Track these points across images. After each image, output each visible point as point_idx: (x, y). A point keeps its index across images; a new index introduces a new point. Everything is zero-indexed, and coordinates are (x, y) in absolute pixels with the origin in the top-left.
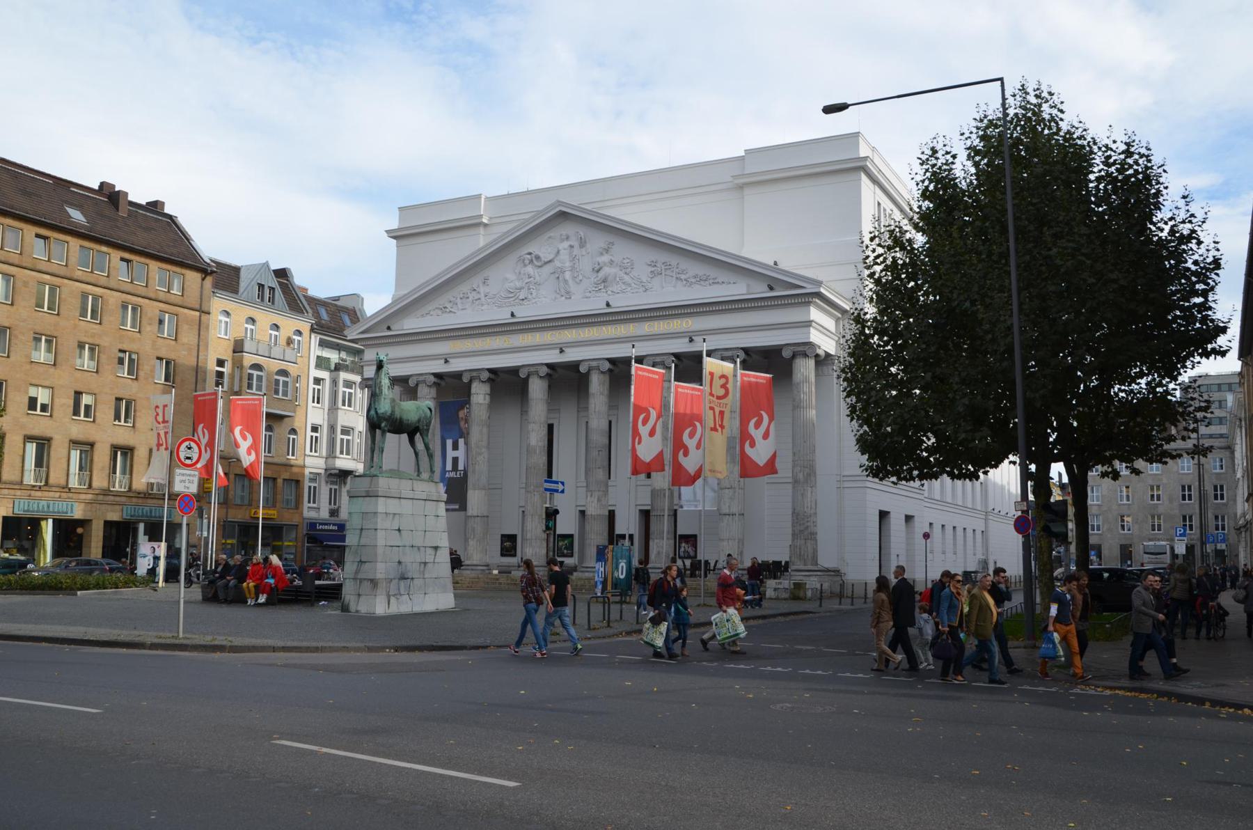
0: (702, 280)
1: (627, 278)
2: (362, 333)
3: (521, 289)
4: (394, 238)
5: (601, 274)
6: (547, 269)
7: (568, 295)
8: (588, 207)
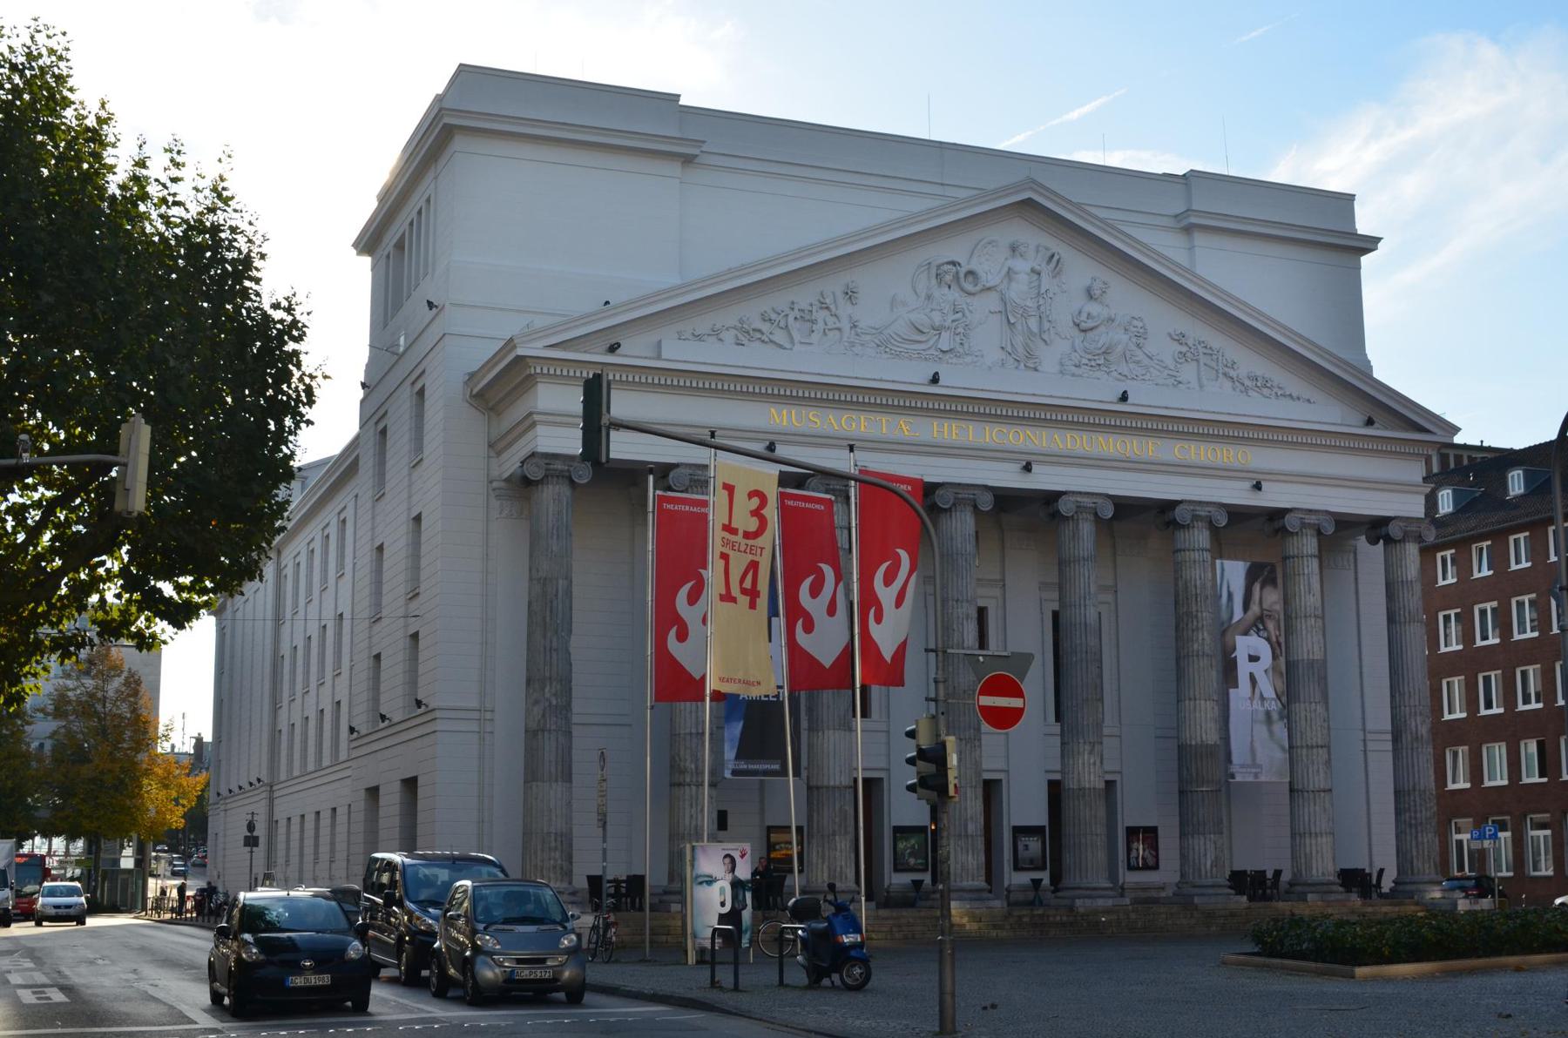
0: (1262, 385)
3: (938, 330)
5: (1103, 338)
6: (991, 302)
7: (1028, 361)
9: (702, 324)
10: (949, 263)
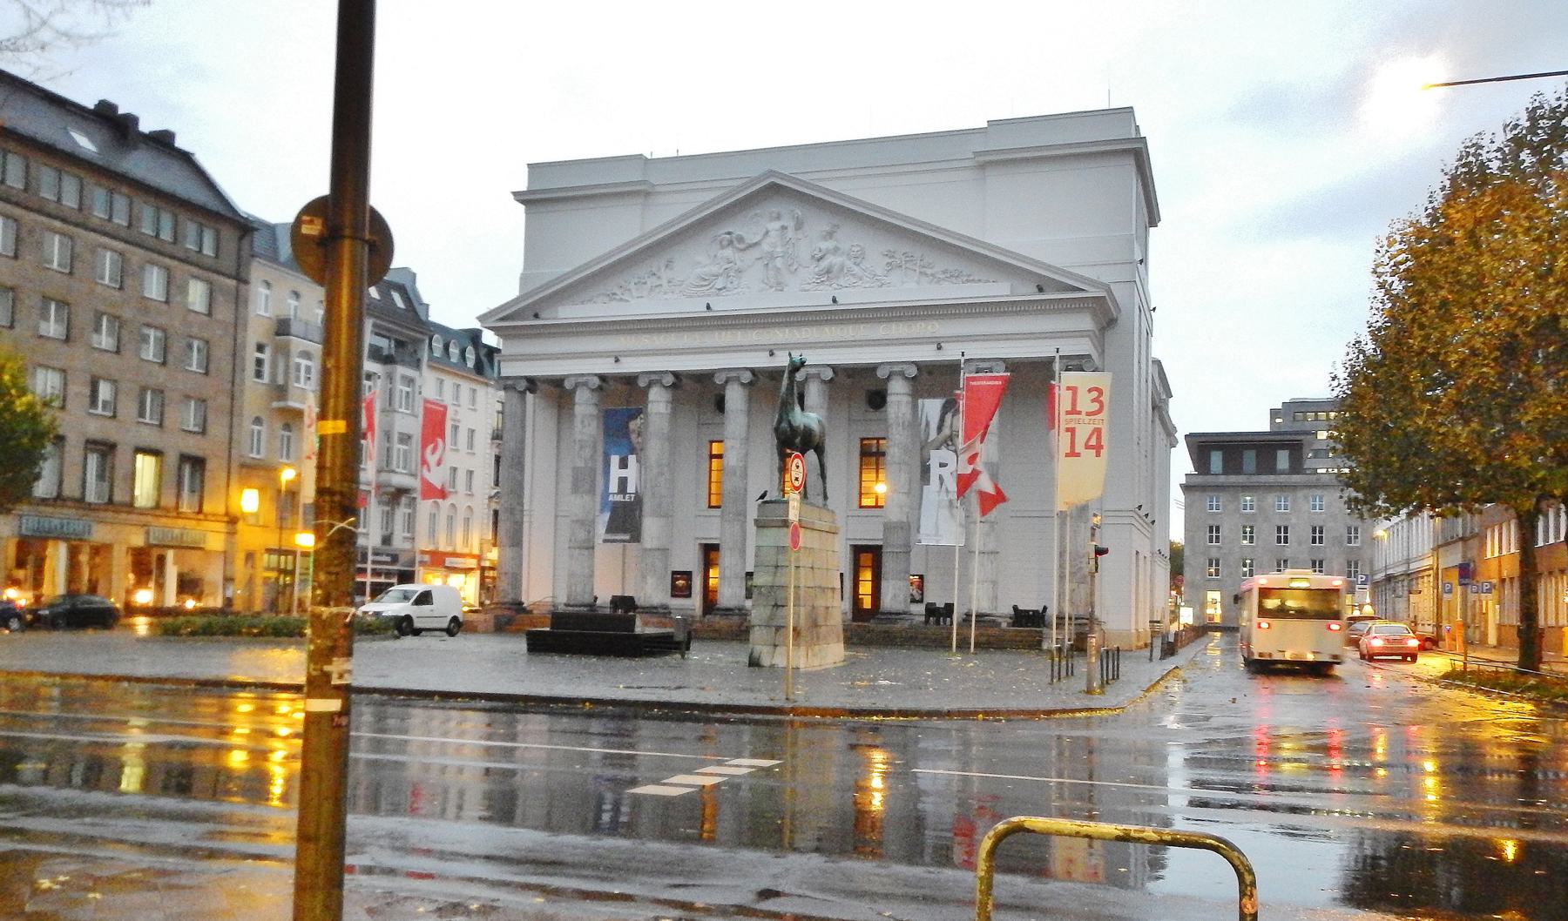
0: (953, 276)
1: (856, 269)
2: (502, 319)
4: (522, 202)
5: (824, 264)
6: (755, 253)
7: (780, 286)
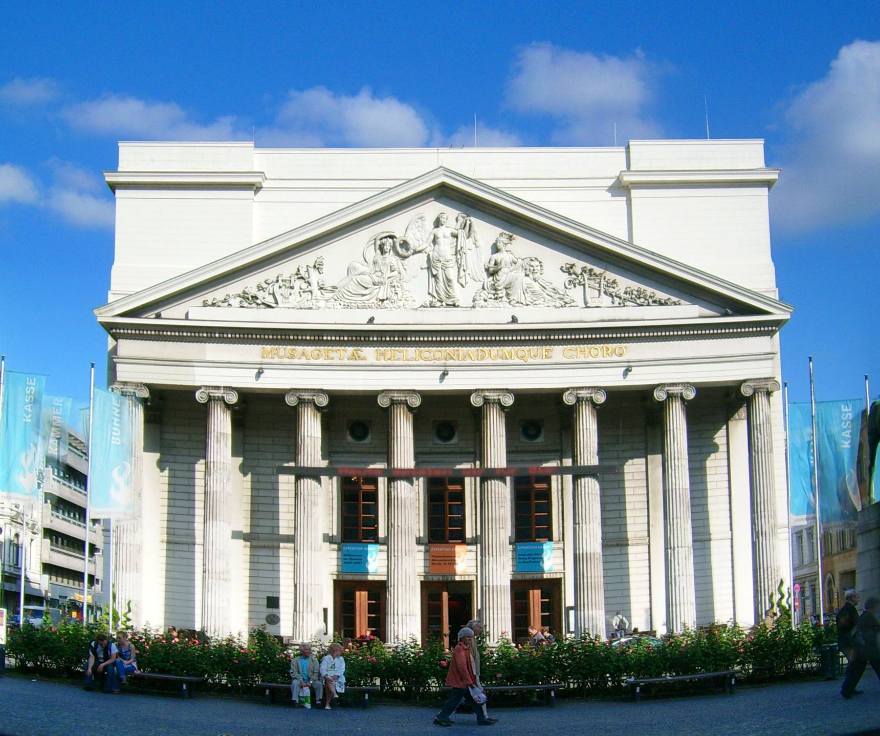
8: (494, 184)
9: (218, 294)
10: (386, 237)
